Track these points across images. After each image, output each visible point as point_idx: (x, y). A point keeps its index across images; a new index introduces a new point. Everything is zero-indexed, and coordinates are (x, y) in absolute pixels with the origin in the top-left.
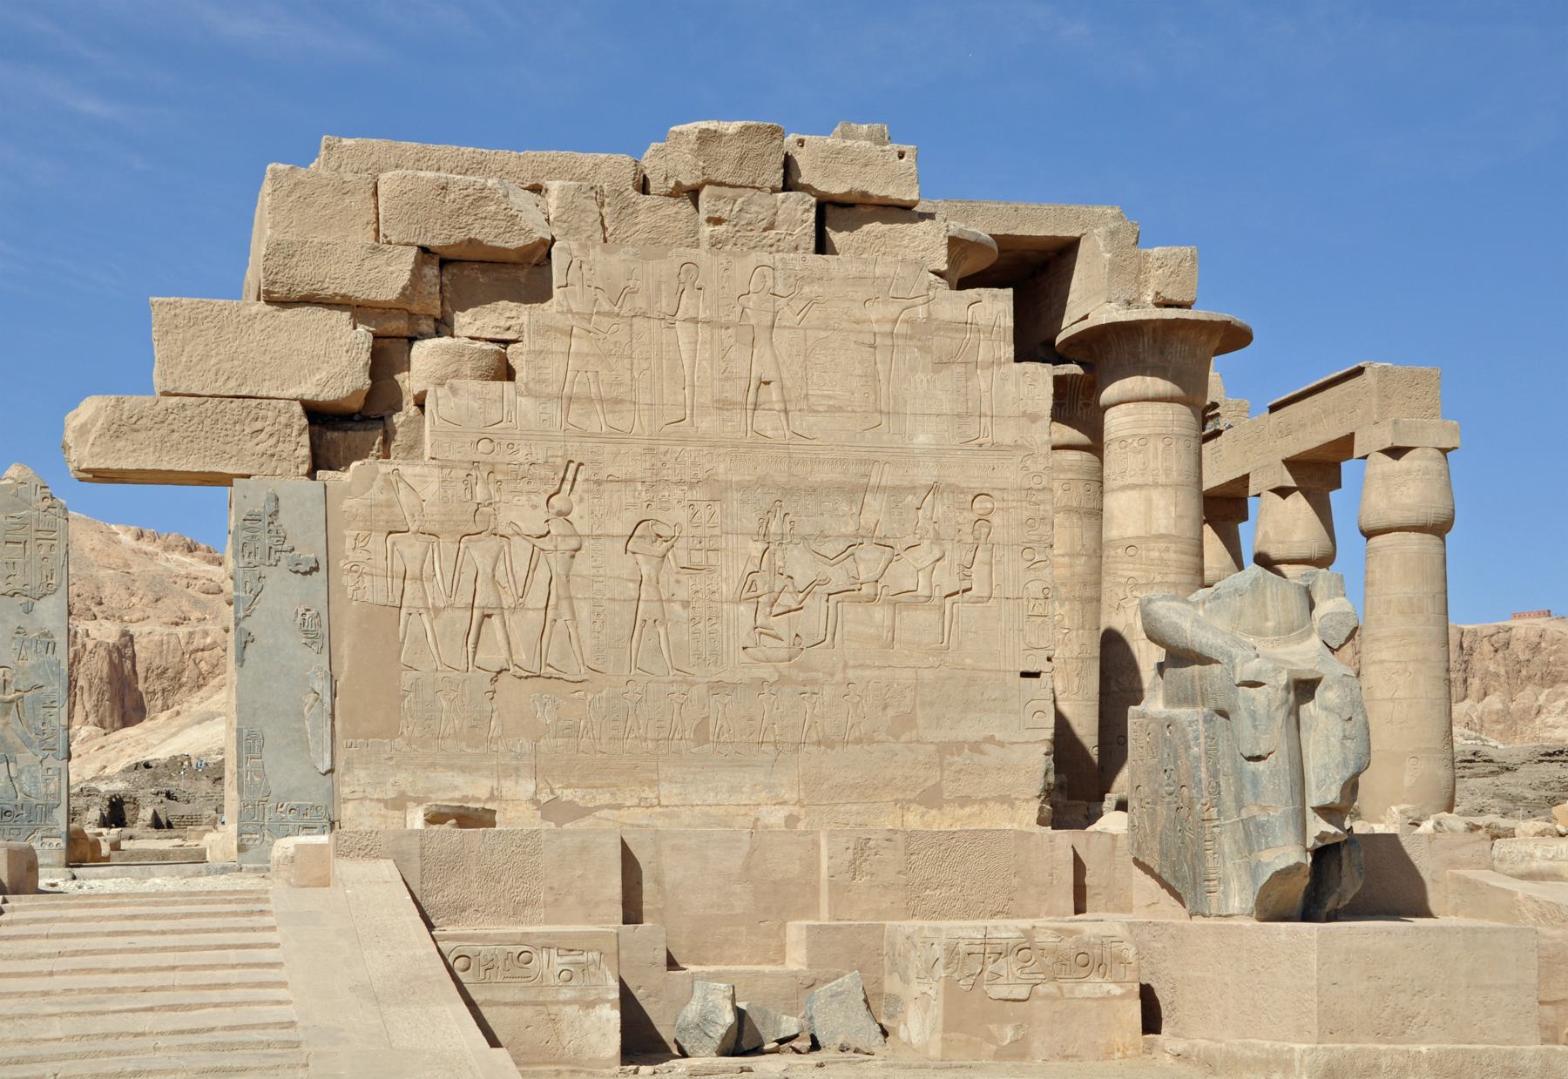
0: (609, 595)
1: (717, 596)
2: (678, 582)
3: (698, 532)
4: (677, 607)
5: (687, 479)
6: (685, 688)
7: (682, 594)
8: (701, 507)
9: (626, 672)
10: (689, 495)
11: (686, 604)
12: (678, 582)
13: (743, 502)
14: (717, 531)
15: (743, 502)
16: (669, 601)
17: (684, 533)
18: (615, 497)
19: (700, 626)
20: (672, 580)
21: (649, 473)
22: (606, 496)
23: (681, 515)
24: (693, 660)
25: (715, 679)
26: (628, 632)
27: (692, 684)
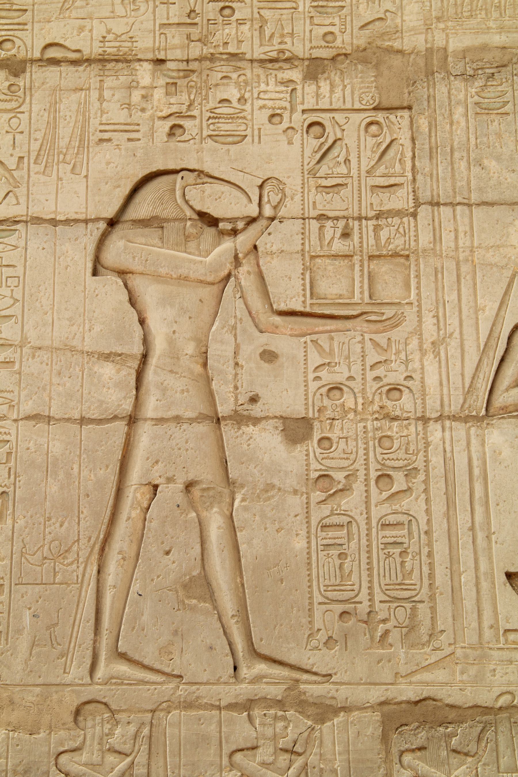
0: (28, 407)
1: (406, 403)
2: (269, 356)
3: (335, 204)
4: (265, 441)
5: (299, 49)
6: (295, 726)
7: (285, 395)
8: (351, 130)
9: (77, 671)
10: (308, 95)
11: (296, 430)
12: (269, 356)
13: (483, 110)
14: (400, 200)
15: (483, 110)
16: (240, 419)
17: (292, 207)
18: (69, 104)
19: (352, 502)
20: (250, 350)
21: (176, 37)
22: (38, 104)
23: (284, 156)
24: (325, 619)
25: (409, 692)
26: (90, 526)
27: (325, 711)
